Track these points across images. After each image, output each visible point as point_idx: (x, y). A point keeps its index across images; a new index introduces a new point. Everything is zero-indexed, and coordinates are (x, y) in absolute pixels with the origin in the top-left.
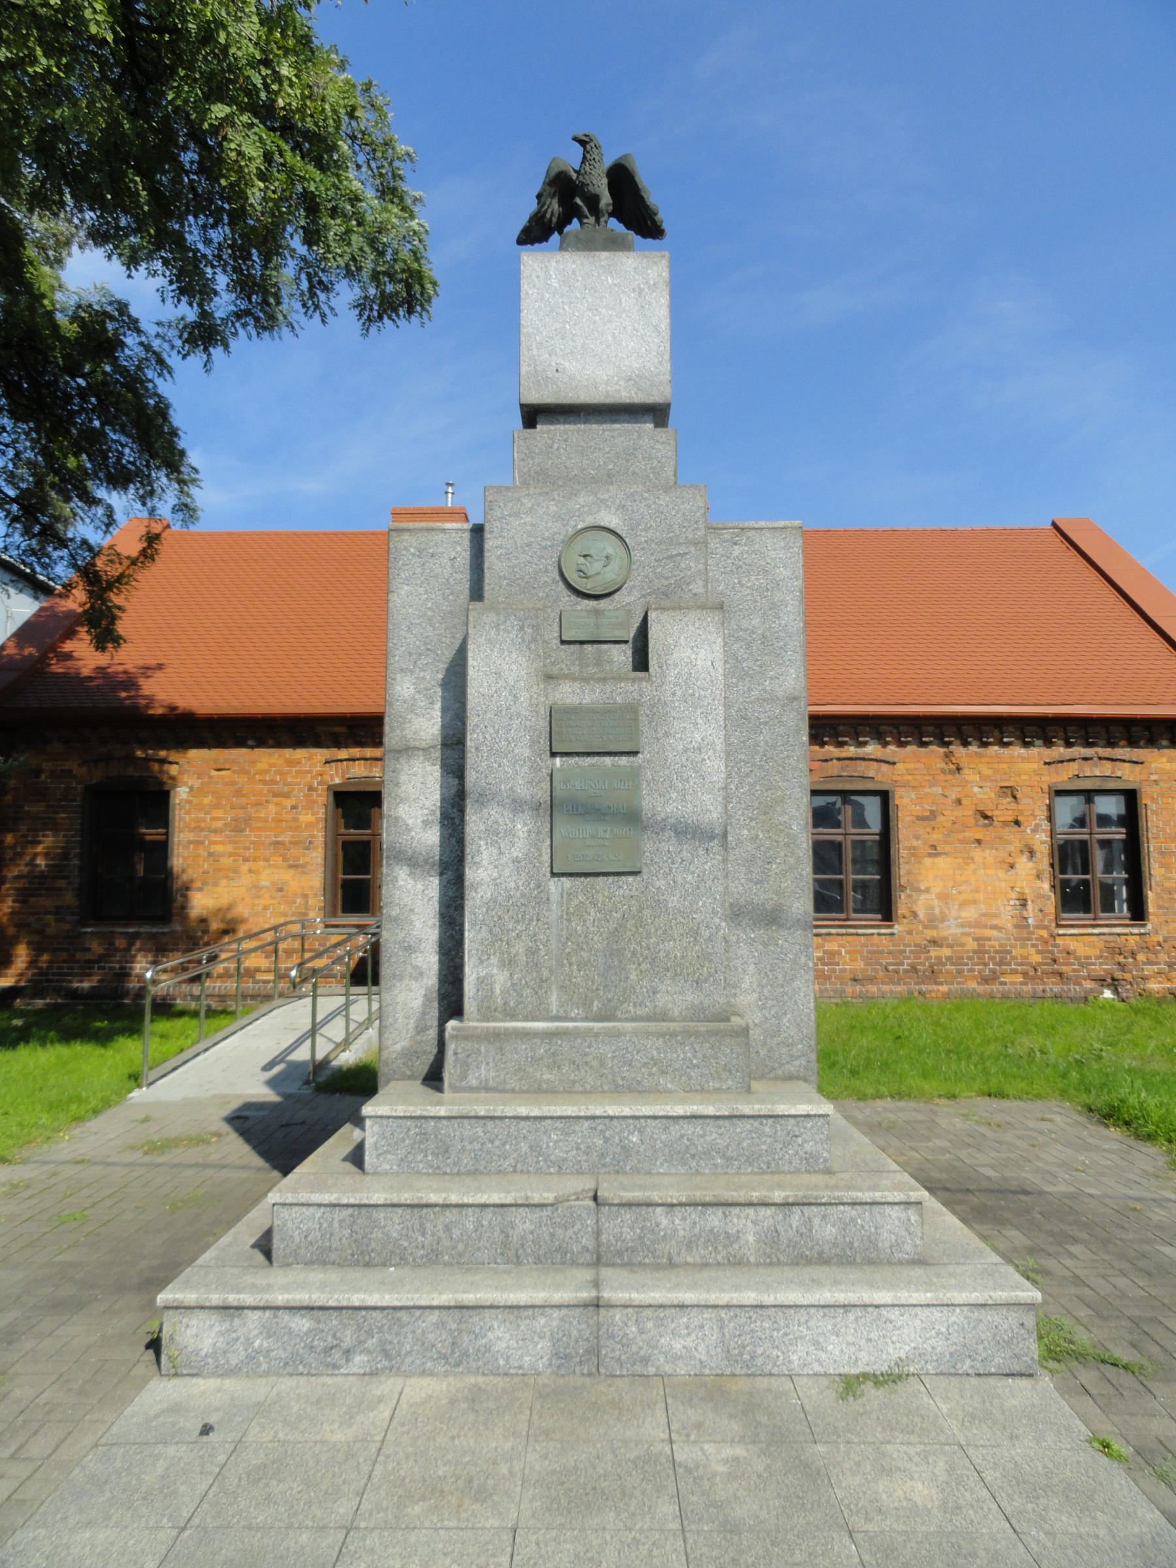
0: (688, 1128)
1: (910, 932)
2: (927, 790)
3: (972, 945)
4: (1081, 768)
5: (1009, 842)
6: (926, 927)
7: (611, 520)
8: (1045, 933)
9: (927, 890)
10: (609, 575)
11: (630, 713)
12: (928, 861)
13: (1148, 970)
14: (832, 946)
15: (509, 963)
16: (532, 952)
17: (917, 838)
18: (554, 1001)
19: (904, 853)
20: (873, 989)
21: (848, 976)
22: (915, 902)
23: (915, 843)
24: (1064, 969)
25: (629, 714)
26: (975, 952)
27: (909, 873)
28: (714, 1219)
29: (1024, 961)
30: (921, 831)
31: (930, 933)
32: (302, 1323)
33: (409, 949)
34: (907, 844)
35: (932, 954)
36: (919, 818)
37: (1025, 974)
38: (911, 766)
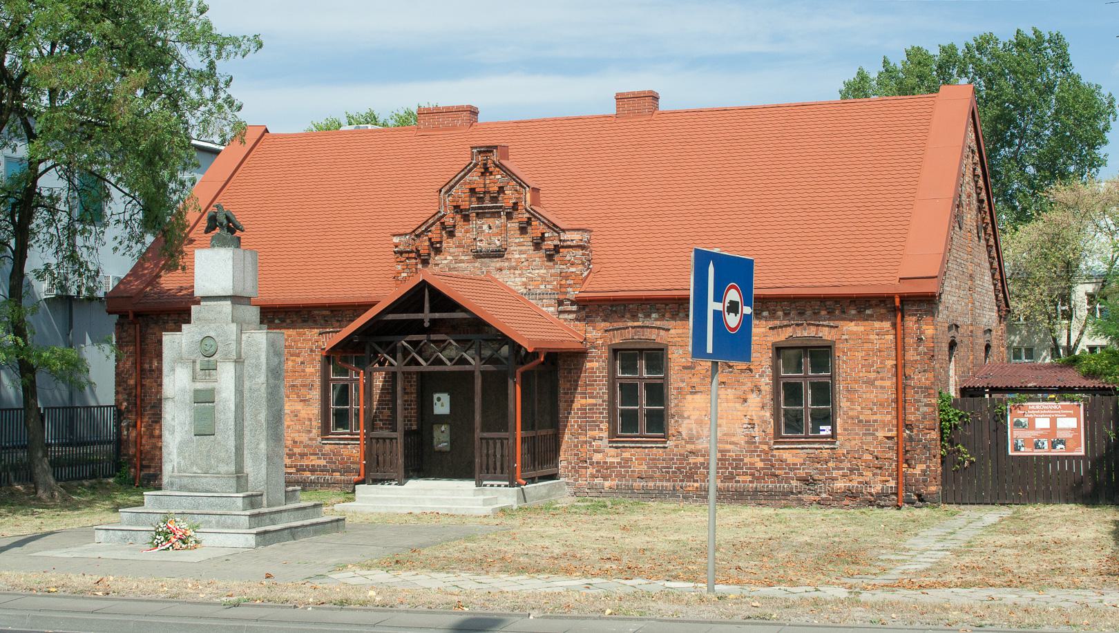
1: (676, 446)
4: (794, 332)
5: (743, 384)
6: (687, 443)
7: (212, 334)
8: (766, 447)
9: (689, 418)
10: (212, 350)
12: (689, 397)
13: (835, 473)
14: (626, 455)
15: (184, 458)
17: (683, 381)
19: (674, 392)
20: (651, 484)
21: (636, 474)
22: (680, 425)
23: (682, 385)
24: (777, 472)
25: (212, 391)
27: (677, 405)
29: (752, 466)
30: (686, 377)
31: (690, 447)
36: (685, 368)
37: (752, 475)
38: (680, 331)
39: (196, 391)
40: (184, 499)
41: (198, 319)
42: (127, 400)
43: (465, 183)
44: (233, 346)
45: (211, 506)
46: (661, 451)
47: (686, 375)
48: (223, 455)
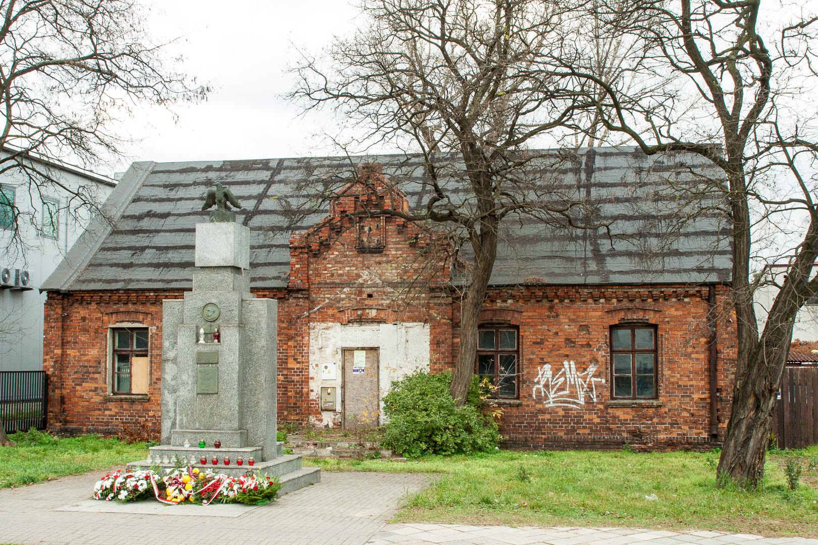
2: (540, 327)
3: (561, 413)
4: (626, 315)
5: (584, 356)
7: (214, 301)
8: (601, 407)
10: (215, 315)
11: (217, 353)
13: (659, 427)
16: (192, 413)
17: (533, 353)
18: (197, 426)
19: (525, 362)
23: (531, 357)
24: (612, 426)
26: (563, 416)
27: (528, 373)
29: (590, 421)
30: (535, 350)
31: (539, 406)
33: (168, 412)
34: (528, 357)
35: (540, 417)
36: (535, 343)
37: (591, 428)
38: (531, 314)
39: (199, 354)
41: (200, 287)
42: (53, 367)
44: (236, 312)
46: (514, 410)
47: (536, 349)
48: (225, 412)
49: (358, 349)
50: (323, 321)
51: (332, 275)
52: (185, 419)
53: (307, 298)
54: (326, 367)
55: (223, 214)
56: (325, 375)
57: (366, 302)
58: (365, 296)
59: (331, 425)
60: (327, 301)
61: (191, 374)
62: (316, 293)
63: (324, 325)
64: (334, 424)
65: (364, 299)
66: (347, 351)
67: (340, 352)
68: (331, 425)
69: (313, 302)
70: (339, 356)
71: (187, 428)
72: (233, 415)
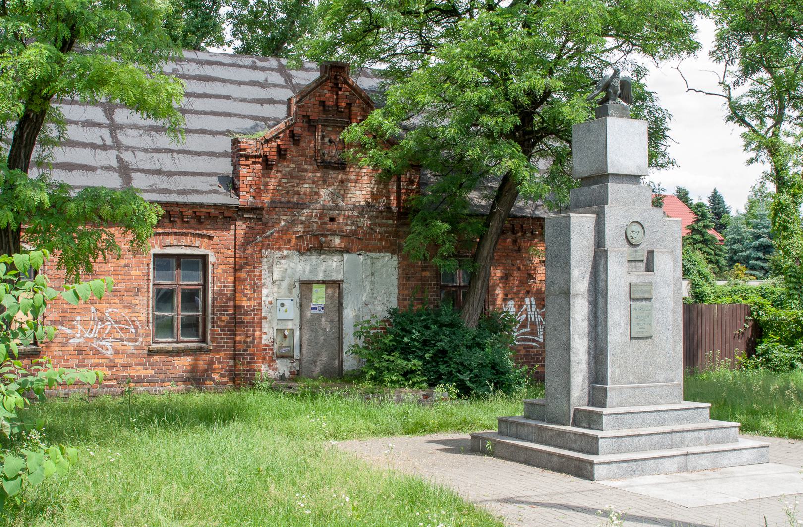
0: (679, 412)
3: (523, 351)
11: (650, 286)
16: (625, 363)
18: (631, 379)
26: (525, 355)
28: (696, 434)
32: (625, 465)
33: (579, 363)
40: (648, 415)
43: (315, 95)
45: (678, 420)
49: (318, 282)
50: (279, 249)
51: (288, 193)
52: (617, 371)
53: (260, 220)
54: (282, 305)
55: (624, 108)
56: (282, 315)
57: (328, 227)
58: (327, 220)
59: (287, 374)
60: (283, 223)
61: (623, 312)
62: (269, 214)
63: (278, 254)
64: (291, 373)
65: (326, 224)
66: (306, 285)
67: (297, 285)
68: (287, 374)
69: (265, 225)
70: (296, 291)
71: (620, 383)
72: (668, 362)
